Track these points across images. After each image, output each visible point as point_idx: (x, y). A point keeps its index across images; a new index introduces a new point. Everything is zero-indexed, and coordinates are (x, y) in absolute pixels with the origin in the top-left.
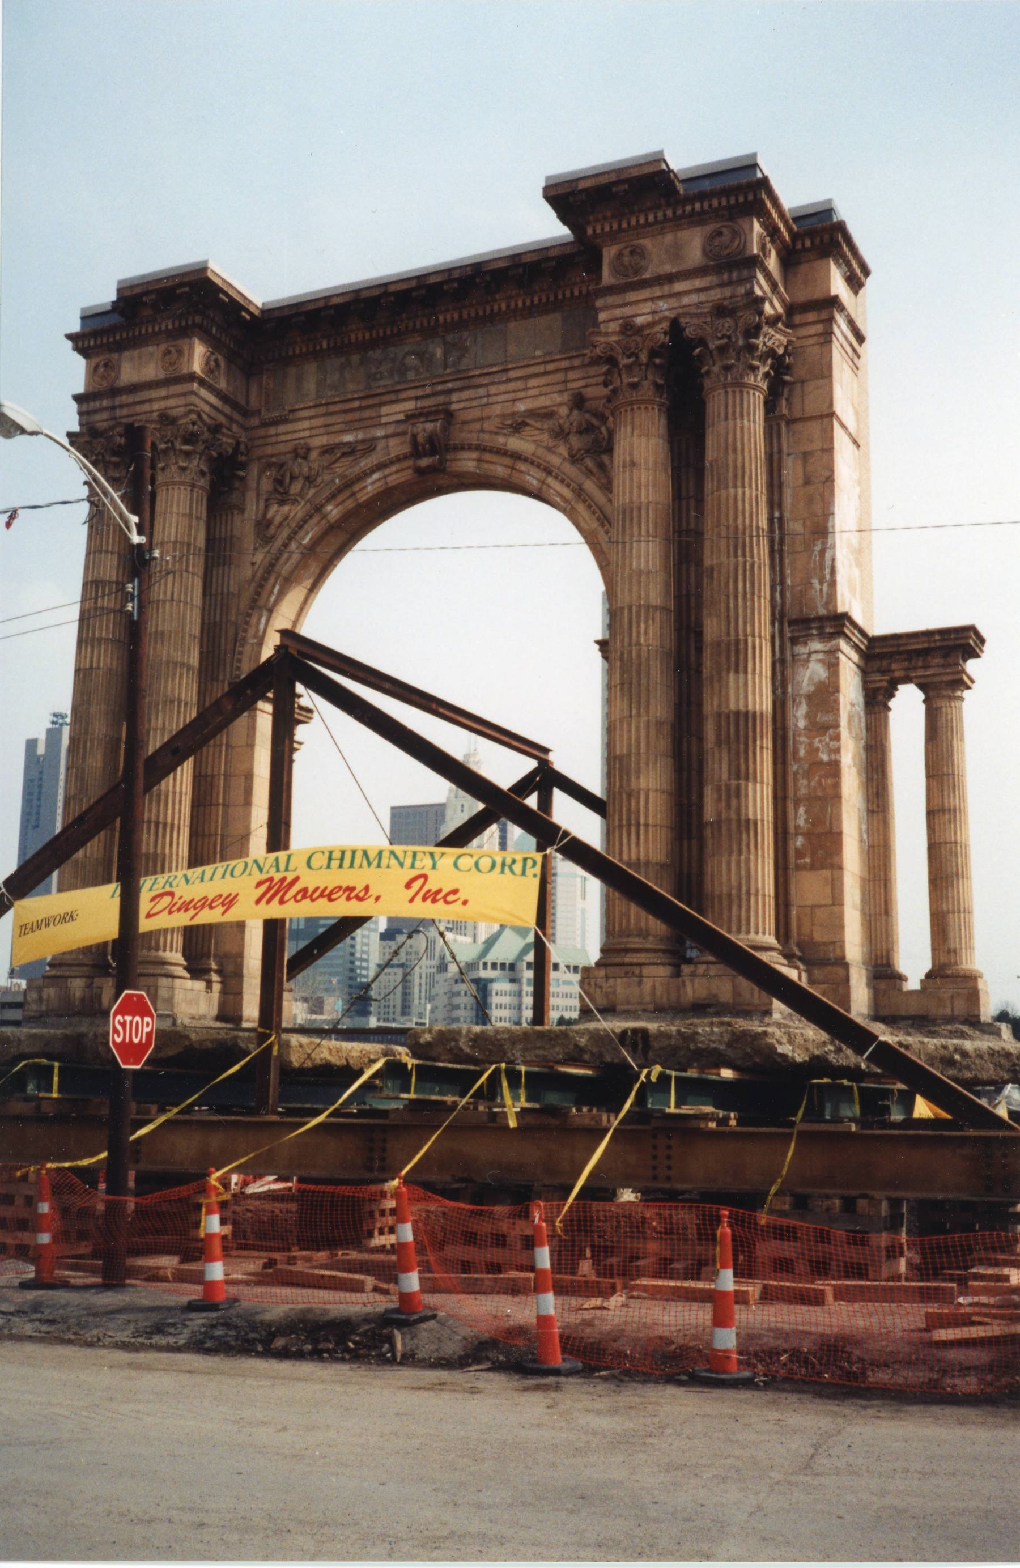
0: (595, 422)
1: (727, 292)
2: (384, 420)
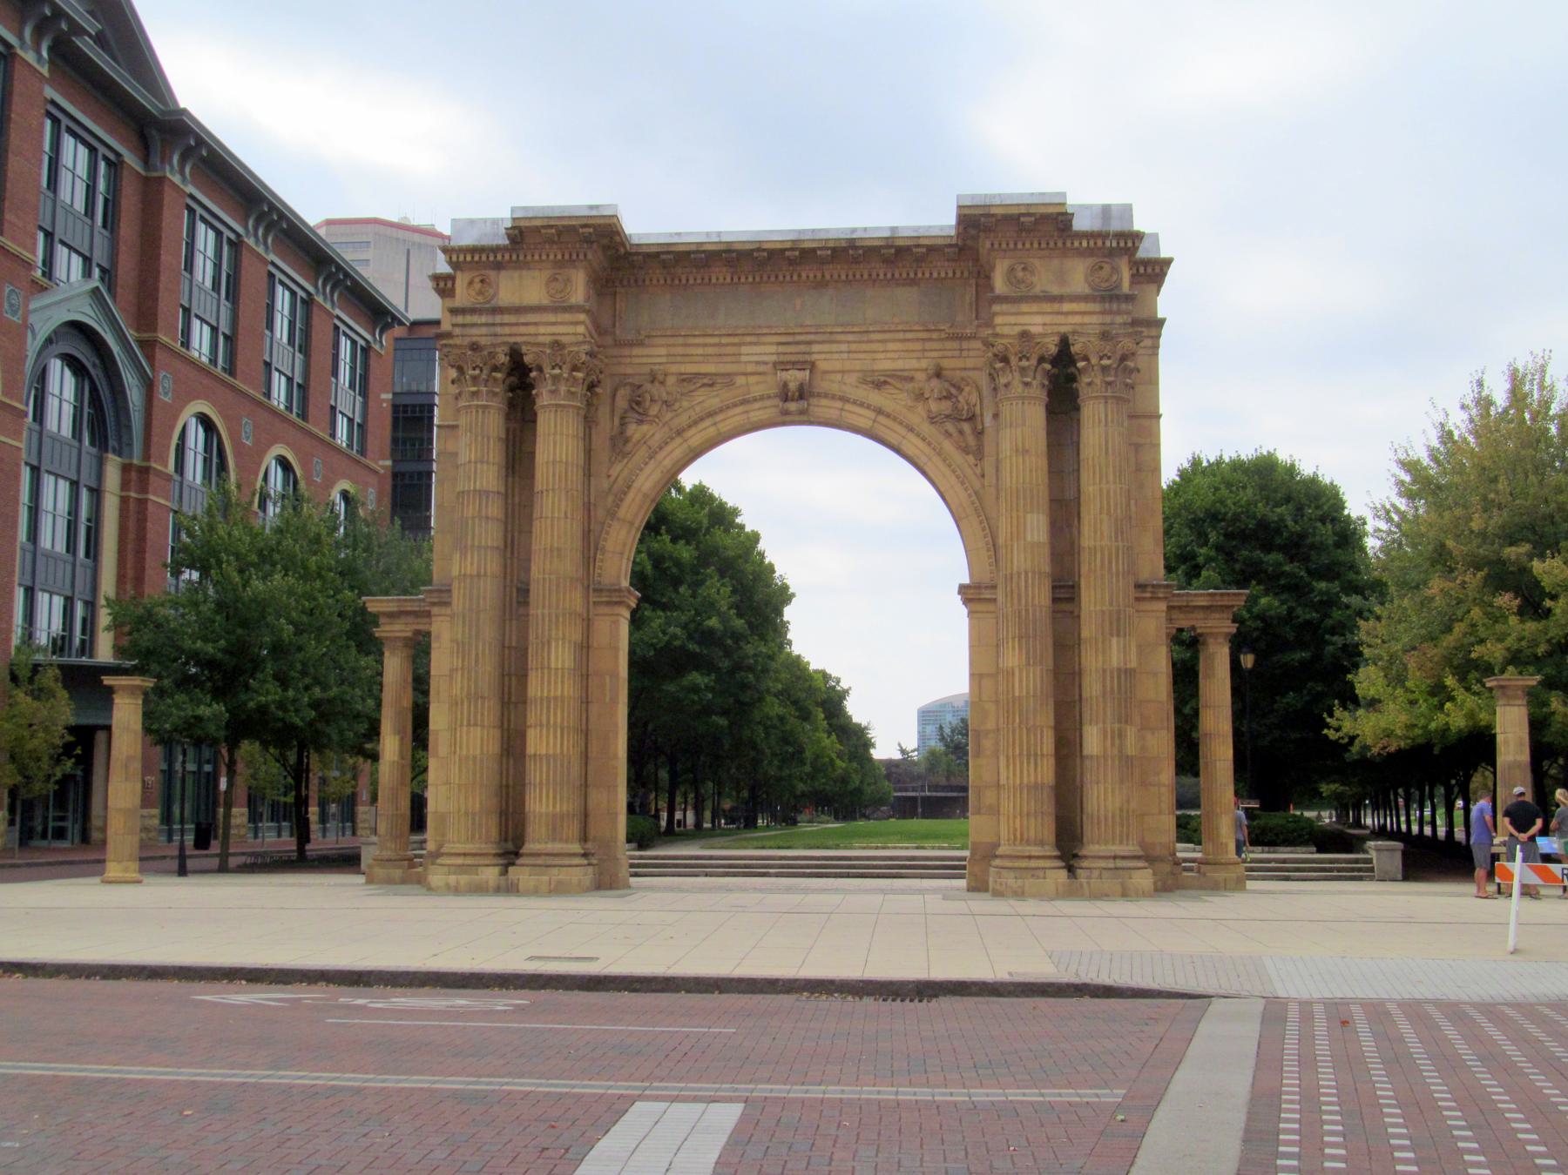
0: (953, 391)
1: (1108, 319)
2: (744, 359)
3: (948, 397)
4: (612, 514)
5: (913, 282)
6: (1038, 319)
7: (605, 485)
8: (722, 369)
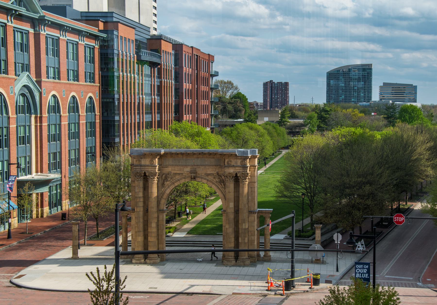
3: (219, 178)
4: (162, 197)
5: (214, 158)
6: (232, 170)
7: (161, 192)
8: (181, 172)
